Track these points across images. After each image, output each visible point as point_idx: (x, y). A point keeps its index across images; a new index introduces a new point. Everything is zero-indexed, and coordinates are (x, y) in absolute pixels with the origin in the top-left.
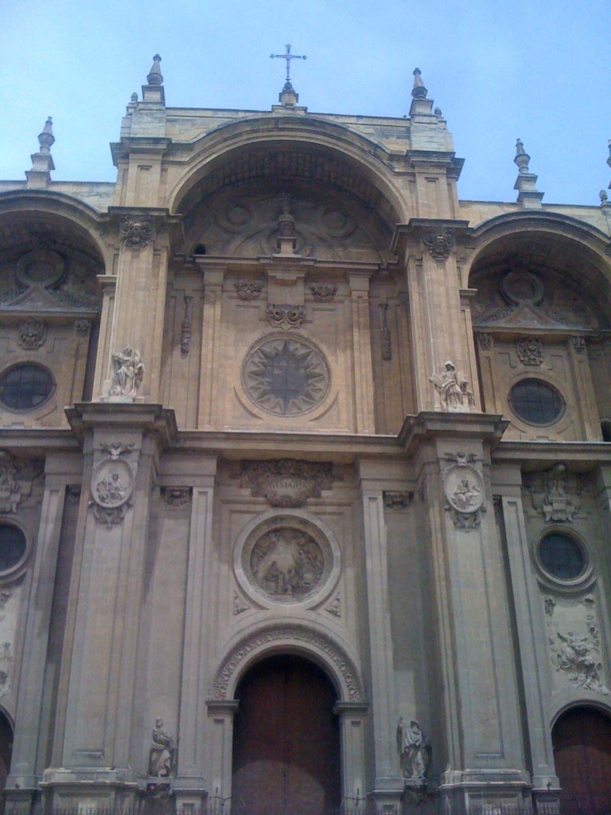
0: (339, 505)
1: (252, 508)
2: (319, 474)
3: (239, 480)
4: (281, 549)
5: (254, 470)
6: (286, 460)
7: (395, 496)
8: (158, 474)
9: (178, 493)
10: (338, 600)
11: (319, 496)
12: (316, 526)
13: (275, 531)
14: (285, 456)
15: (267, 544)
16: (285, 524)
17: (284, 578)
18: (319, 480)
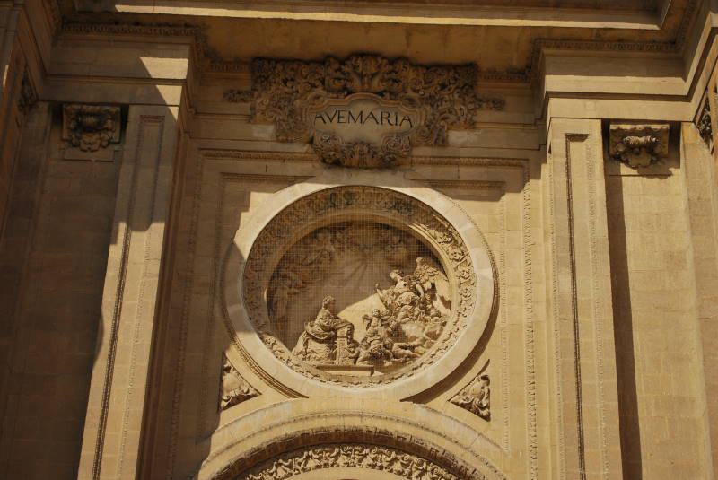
0: (493, 163)
1: (275, 168)
2: (445, 94)
3: (248, 105)
4: (348, 271)
5: (285, 82)
6: (362, 55)
7: (633, 133)
8: (45, 74)
9: (91, 120)
10: (485, 378)
11: (442, 142)
12: (433, 211)
13: (336, 228)
14: (361, 43)
15: (313, 257)
16: (359, 212)
17: (351, 333)
18: (445, 105)
